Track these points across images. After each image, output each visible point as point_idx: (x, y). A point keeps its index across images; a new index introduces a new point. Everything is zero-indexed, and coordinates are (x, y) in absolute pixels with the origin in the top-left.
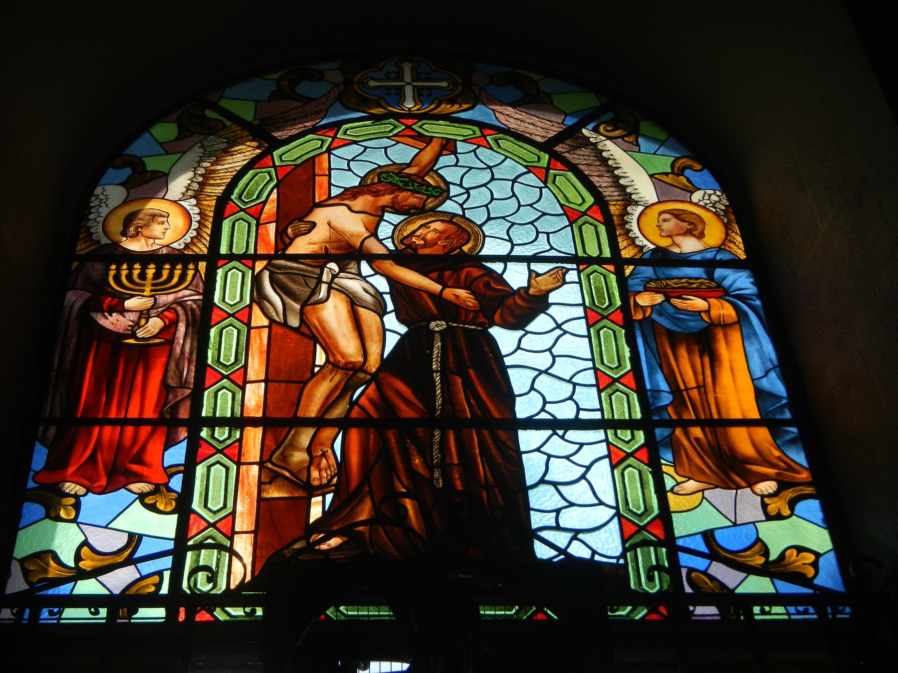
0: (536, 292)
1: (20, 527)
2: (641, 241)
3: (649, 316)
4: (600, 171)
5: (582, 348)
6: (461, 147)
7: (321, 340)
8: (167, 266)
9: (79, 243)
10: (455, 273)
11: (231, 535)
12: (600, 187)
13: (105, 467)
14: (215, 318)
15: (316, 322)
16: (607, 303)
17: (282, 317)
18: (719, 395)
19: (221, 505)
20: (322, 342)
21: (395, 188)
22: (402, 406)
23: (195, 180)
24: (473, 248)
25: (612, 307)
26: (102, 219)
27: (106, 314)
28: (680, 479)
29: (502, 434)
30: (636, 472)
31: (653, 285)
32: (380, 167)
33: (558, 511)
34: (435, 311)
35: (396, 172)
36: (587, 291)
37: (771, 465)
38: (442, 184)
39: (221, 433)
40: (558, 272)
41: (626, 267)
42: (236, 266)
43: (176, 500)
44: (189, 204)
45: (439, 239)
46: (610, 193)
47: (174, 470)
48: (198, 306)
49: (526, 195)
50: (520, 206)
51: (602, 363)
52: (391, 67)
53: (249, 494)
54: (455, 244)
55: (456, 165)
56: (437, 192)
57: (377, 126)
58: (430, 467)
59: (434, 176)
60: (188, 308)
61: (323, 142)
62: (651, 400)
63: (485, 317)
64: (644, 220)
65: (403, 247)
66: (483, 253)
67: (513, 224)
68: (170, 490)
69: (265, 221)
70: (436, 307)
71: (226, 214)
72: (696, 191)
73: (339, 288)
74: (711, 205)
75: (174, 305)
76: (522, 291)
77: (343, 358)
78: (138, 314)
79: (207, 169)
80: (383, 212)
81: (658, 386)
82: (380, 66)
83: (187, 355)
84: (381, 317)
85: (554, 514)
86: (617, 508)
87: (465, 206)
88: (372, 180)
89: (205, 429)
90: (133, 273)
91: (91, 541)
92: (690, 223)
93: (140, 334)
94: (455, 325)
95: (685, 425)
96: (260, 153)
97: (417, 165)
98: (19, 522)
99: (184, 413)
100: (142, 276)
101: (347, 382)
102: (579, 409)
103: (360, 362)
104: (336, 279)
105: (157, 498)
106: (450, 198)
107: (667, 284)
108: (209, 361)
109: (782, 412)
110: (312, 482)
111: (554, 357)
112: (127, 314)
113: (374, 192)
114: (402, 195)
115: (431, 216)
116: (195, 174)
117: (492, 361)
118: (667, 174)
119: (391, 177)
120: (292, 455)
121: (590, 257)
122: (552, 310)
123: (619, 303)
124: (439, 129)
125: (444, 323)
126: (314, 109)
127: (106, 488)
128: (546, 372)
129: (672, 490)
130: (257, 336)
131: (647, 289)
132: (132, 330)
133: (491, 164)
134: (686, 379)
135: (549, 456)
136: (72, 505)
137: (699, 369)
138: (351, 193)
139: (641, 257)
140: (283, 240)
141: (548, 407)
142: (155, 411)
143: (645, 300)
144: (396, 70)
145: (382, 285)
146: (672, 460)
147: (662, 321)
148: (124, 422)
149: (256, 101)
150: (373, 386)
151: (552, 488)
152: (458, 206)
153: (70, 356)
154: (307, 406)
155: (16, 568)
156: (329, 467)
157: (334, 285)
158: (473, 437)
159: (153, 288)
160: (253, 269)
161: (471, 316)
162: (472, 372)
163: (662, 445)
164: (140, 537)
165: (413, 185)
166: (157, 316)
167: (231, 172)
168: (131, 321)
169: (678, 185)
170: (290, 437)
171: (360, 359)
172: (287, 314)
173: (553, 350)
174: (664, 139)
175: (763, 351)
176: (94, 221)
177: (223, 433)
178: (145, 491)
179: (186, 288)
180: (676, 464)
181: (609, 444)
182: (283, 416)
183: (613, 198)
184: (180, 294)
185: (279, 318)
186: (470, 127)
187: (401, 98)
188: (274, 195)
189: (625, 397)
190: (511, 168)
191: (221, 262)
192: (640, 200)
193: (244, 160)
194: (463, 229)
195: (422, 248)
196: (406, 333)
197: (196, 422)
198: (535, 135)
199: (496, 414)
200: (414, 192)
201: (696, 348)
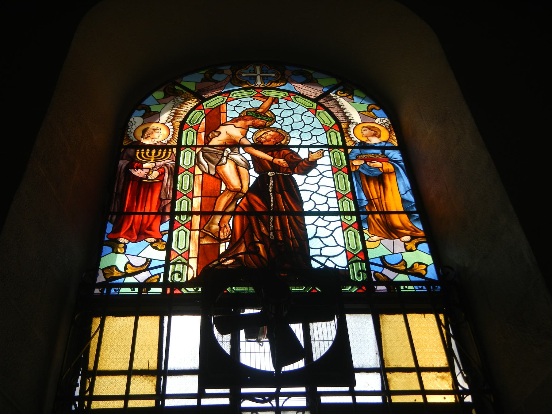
2: (355, 139)
3: (358, 170)
5: (331, 182)
6: (281, 101)
7: (224, 180)
8: (160, 150)
9: (124, 141)
10: (278, 153)
11: (188, 259)
13: (136, 232)
15: (222, 173)
16: (341, 164)
17: (207, 171)
18: (386, 201)
19: (184, 247)
20: (224, 181)
21: (253, 118)
22: (257, 206)
23: (171, 115)
26: (133, 131)
27: (136, 170)
28: (371, 235)
29: (298, 217)
30: (353, 233)
31: (359, 157)
32: (247, 109)
33: (321, 249)
34: (270, 168)
36: (332, 159)
37: (408, 230)
38: (273, 116)
39: (183, 218)
42: (189, 150)
43: (165, 245)
45: (272, 138)
46: (342, 119)
47: (164, 233)
48: (173, 166)
49: (308, 120)
50: (305, 125)
51: (339, 188)
52: (251, 68)
53: (195, 242)
54: (278, 141)
55: (278, 108)
56: (270, 119)
58: (269, 231)
60: (169, 167)
61: (224, 99)
62: (359, 204)
65: (257, 142)
66: (290, 144)
67: (302, 132)
69: (200, 132)
70: (271, 166)
74: (383, 124)
75: (163, 166)
78: (149, 170)
81: (362, 198)
82: (247, 68)
83: (169, 186)
84: (248, 170)
86: (345, 247)
87: (282, 125)
89: (177, 216)
90: (146, 153)
91: (131, 261)
92: (375, 131)
93: (150, 178)
94: (278, 173)
95: (373, 213)
96: (198, 104)
98: (101, 254)
99: (168, 210)
100: (150, 154)
102: (329, 207)
103: (240, 189)
106: (276, 122)
107: (365, 156)
108: (178, 189)
109: (413, 208)
110: (221, 237)
111: (319, 186)
112: (144, 170)
113: (245, 119)
114: (256, 121)
115: (268, 129)
116: (171, 112)
117: (294, 188)
118: (365, 111)
119: (252, 113)
120: (212, 227)
121: (334, 146)
122: (318, 167)
123: (345, 164)
124: (271, 94)
125: (274, 173)
127: (137, 240)
128: (316, 192)
129: (367, 240)
130: (197, 178)
131: (357, 159)
132: (146, 176)
135: (317, 227)
136: (123, 247)
138: (235, 120)
140: (208, 139)
142: (156, 209)
143: (356, 163)
144: (253, 69)
145: (248, 157)
146: (367, 228)
147: (363, 171)
148: (144, 213)
149: (196, 82)
151: (318, 239)
152: (279, 125)
153: (121, 187)
154: (218, 207)
155: (100, 272)
156: (228, 231)
157: (228, 158)
158: (286, 219)
159: (154, 159)
160: (195, 151)
161: (285, 170)
162: (285, 192)
164: (151, 260)
165: (261, 117)
167: (186, 111)
169: (370, 116)
170: (211, 219)
174: (364, 97)
175: (405, 184)
177: (184, 218)
178: (153, 241)
179: (168, 159)
181: (342, 221)
182: (208, 211)
184: (166, 162)
185: (206, 171)
186: (284, 92)
187: (256, 81)
188: (204, 121)
189: (348, 202)
190: (301, 109)
191: (182, 148)
194: (282, 134)
197: (173, 213)
199: (295, 210)
200: (261, 119)
201: (377, 182)
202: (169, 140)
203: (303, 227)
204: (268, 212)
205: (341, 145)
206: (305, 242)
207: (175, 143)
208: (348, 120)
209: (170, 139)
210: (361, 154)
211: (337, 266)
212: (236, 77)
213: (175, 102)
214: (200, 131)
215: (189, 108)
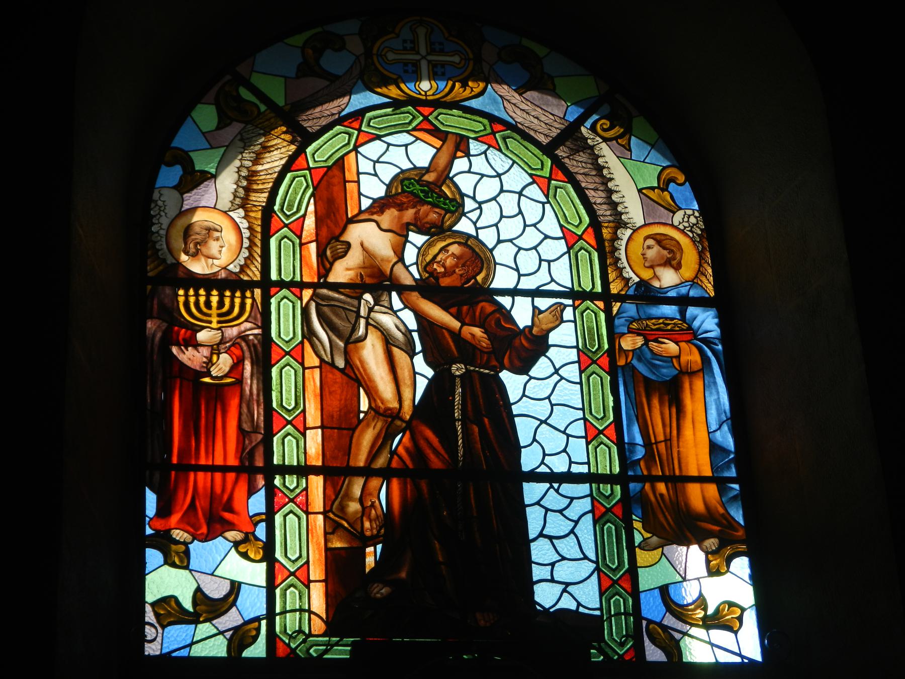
0: (538, 332)
1: (147, 572)
2: (628, 273)
3: (630, 362)
4: (595, 183)
6: (475, 147)
7: (363, 383)
9: (149, 261)
10: (471, 309)
11: (307, 583)
12: (595, 203)
13: (204, 515)
14: (274, 357)
16: (597, 346)
17: (330, 356)
18: (681, 449)
19: (297, 555)
20: (365, 386)
22: (432, 457)
23: (240, 184)
24: (486, 279)
25: (600, 350)
27: (182, 347)
31: (635, 326)
32: (403, 171)
33: (553, 565)
34: (456, 352)
35: (417, 179)
36: (581, 331)
37: (716, 522)
38: (457, 196)
39: (291, 481)
40: (557, 308)
41: (614, 303)
42: (287, 295)
43: (263, 548)
44: (237, 215)
45: (456, 266)
46: (603, 211)
47: (258, 518)
48: (259, 341)
49: (532, 212)
50: (525, 226)
53: (318, 544)
56: (453, 207)
57: (397, 116)
59: (451, 185)
60: (251, 344)
61: (350, 135)
62: (627, 453)
63: (497, 360)
64: (632, 245)
65: (427, 275)
67: (520, 249)
68: (257, 539)
70: (456, 348)
71: (272, 231)
72: (678, 211)
73: (375, 324)
74: (689, 229)
75: (239, 340)
77: (382, 403)
78: (210, 349)
79: (250, 169)
80: (408, 230)
81: (634, 439)
83: (255, 397)
85: (549, 568)
87: (478, 225)
88: (396, 189)
92: (671, 251)
94: (472, 368)
97: (435, 170)
99: (259, 463)
100: (208, 304)
102: (571, 462)
103: (396, 408)
104: (372, 313)
105: (247, 547)
106: (464, 214)
107: (647, 324)
108: (274, 405)
109: (729, 468)
111: (552, 405)
112: (201, 349)
114: (425, 208)
115: (449, 237)
116: (240, 176)
117: (502, 409)
118: (653, 188)
119: (412, 184)
120: (348, 506)
121: (584, 291)
122: (551, 352)
123: (606, 346)
124: (452, 121)
127: (207, 536)
129: (639, 546)
131: (630, 331)
133: (500, 172)
135: (547, 510)
137: (668, 421)
138: (379, 206)
139: (627, 291)
140: (325, 265)
141: (548, 460)
142: (236, 457)
143: (629, 343)
145: (412, 324)
147: (641, 368)
148: (213, 469)
149: (286, 78)
150: (408, 433)
151: (547, 541)
154: (357, 455)
155: (148, 608)
157: (371, 321)
160: (301, 299)
162: (486, 420)
164: (240, 584)
166: (226, 352)
167: (271, 174)
168: (205, 357)
169: (662, 203)
170: (345, 486)
171: (395, 405)
172: (334, 353)
173: (551, 398)
175: (720, 402)
176: (157, 235)
179: (246, 321)
183: (606, 218)
184: (243, 327)
186: (481, 119)
188: (312, 208)
189: (607, 449)
190: (517, 178)
191: (273, 290)
192: (628, 221)
194: (477, 254)
195: (442, 277)
196: (434, 377)
197: (271, 470)
198: (539, 132)
200: (434, 205)
201: (666, 398)
202: (242, 262)
203: (519, 508)
207: (255, 273)
208: (615, 215)
209: (245, 259)
212: (373, 64)
213: (245, 143)
215: (276, 164)
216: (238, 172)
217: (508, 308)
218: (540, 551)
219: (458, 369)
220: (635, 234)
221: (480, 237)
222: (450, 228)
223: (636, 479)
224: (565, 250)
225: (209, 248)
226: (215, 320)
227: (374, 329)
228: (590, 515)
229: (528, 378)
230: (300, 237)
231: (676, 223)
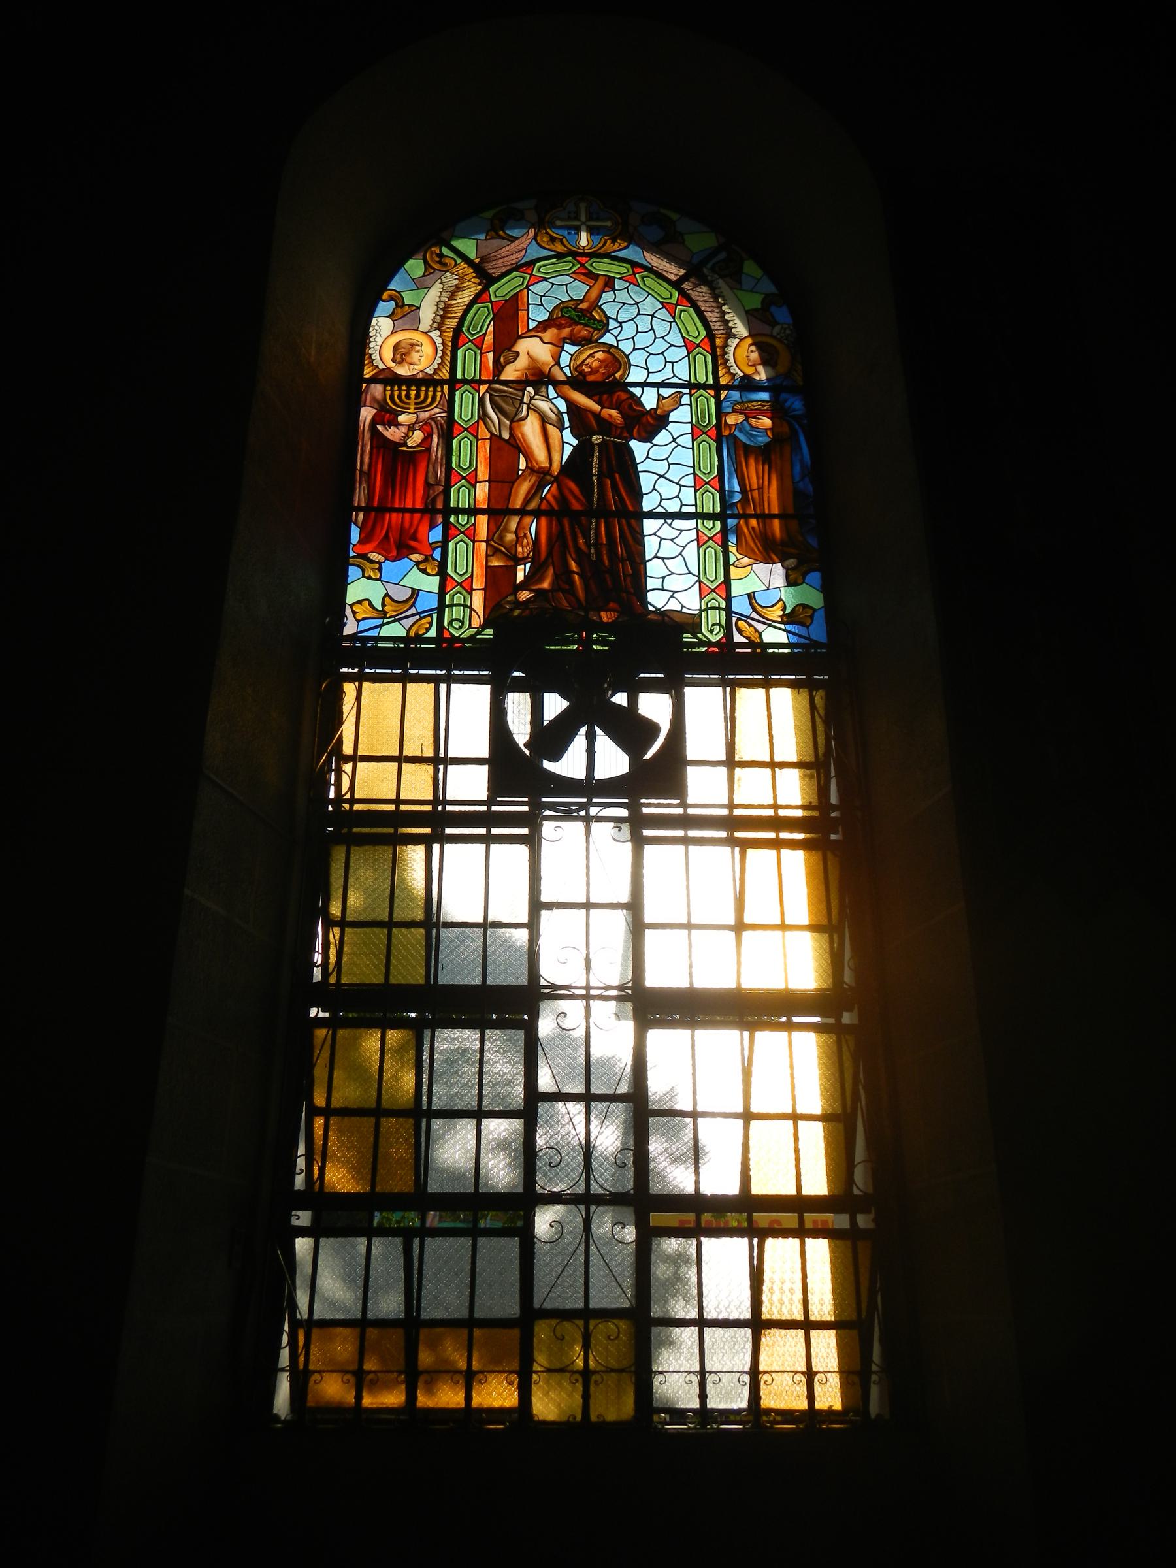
2: (735, 370)
5: (686, 457)
6: (619, 284)
7: (523, 450)
9: (365, 368)
11: (470, 592)
15: (520, 435)
16: (707, 422)
17: (498, 431)
19: (465, 571)
21: (572, 322)
22: (573, 501)
24: (622, 376)
26: (379, 347)
28: (739, 556)
29: (633, 522)
30: (713, 551)
33: (663, 578)
35: (573, 307)
39: (463, 519)
42: (468, 389)
43: (438, 567)
45: (600, 367)
46: (717, 327)
47: (436, 545)
49: (661, 328)
50: (655, 338)
53: (481, 563)
55: (614, 301)
58: (588, 545)
61: (524, 278)
62: (727, 498)
64: (739, 351)
66: (628, 380)
67: (650, 354)
68: (434, 559)
69: (486, 351)
71: (460, 345)
75: (429, 421)
76: (652, 411)
77: (537, 464)
78: (407, 427)
81: (733, 488)
83: (439, 460)
87: (619, 338)
88: (557, 314)
89: (453, 516)
94: (608, 438)
95: (746, 517)
96: (481, 289)
98: (347, 579)
99: (440, 506)
100: (408, 396)
101: (539, 483)
102: (682, 505)
104: (533, 401)
106: (609, 331)
107: (748, 406)
108: (453, 465)
111: (669, 465)
112: (400, 427)
115: (596, 347)
116: (438, 308)
120: (506, 536)
121: (699, 383)
123: (714, 422)
124: (603, 267)
126: (518, 248)
127: (396, 558)
129: (733, 564)
133: (638, 301)
134: (752, 484)
135: (661, 539)
138: (543, 326)
142: (422, 503)
145: (562, 405)
146: (735, 543)
148: (404, 510)
150: (555, 484)
153: (367, 459)
154: (515, 500)
156: (528, 544)
158: (615, 525)
159: (416, 406)
160: (478, 391)
163: (731, 531)
170: (503, 524)
171: (547, 465)
172: (502, 428)
173: (669, 459)
174: (759, 277)
176: (373, 349)
179: (436, 407)
180: (738, 545)
181: (698, 531)
182: (500, 507)
184: (433, 412)
188: (491, 328)
189: (711, 495)
190: (650, 305)
191: (458, 386)
193: (470, 296)
195: (589, 375)
197: (448, 511)
198: (671, 273)
200: (585, 325)
201: (761, 458)
202: (436, 367)
203: (638, 538)
204: (589, 513)
205: (712, 383)
206: (642, 566)
207: (445, 374)
209: (438, 364)
210: (740, 401)
211: (684, 608)
214: (486, 348)
215: (466, 299)
216: (437, 305)
217: (639, 396)
218: (654, 568)
219: (596, 439)
220: (742, 342)
221: (619, 347)
222: (596, 341)
223: (732, 516)
224: (686, 354)
225: (412, 358)
226: (412, 407)
227: (533, 412)
228: (696, 542)
229: (652, 445)
230: (480, 349)
231: (775, 333)
